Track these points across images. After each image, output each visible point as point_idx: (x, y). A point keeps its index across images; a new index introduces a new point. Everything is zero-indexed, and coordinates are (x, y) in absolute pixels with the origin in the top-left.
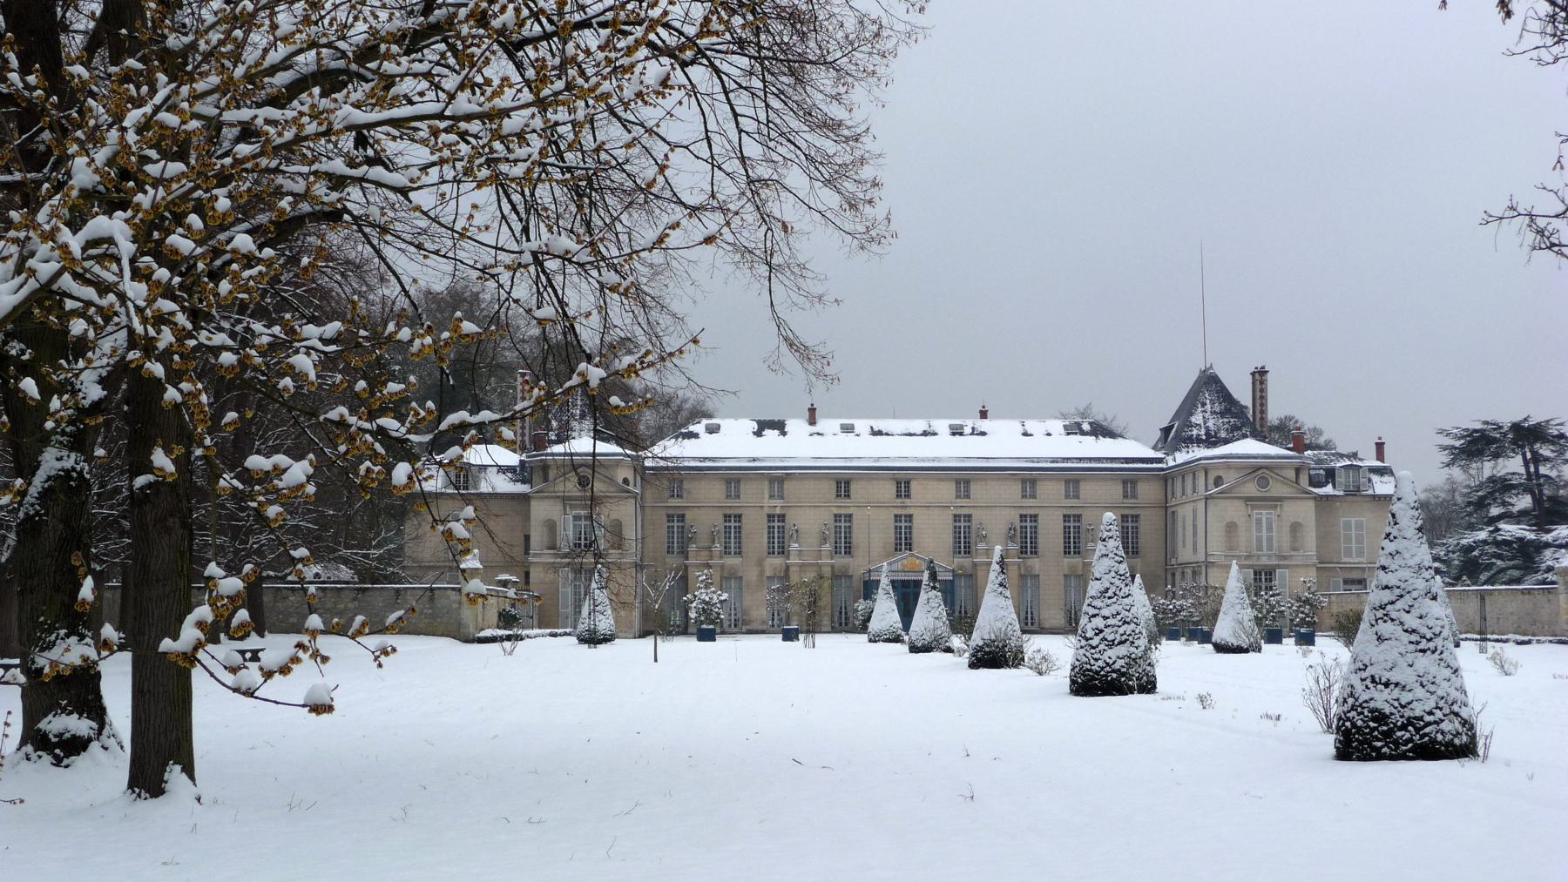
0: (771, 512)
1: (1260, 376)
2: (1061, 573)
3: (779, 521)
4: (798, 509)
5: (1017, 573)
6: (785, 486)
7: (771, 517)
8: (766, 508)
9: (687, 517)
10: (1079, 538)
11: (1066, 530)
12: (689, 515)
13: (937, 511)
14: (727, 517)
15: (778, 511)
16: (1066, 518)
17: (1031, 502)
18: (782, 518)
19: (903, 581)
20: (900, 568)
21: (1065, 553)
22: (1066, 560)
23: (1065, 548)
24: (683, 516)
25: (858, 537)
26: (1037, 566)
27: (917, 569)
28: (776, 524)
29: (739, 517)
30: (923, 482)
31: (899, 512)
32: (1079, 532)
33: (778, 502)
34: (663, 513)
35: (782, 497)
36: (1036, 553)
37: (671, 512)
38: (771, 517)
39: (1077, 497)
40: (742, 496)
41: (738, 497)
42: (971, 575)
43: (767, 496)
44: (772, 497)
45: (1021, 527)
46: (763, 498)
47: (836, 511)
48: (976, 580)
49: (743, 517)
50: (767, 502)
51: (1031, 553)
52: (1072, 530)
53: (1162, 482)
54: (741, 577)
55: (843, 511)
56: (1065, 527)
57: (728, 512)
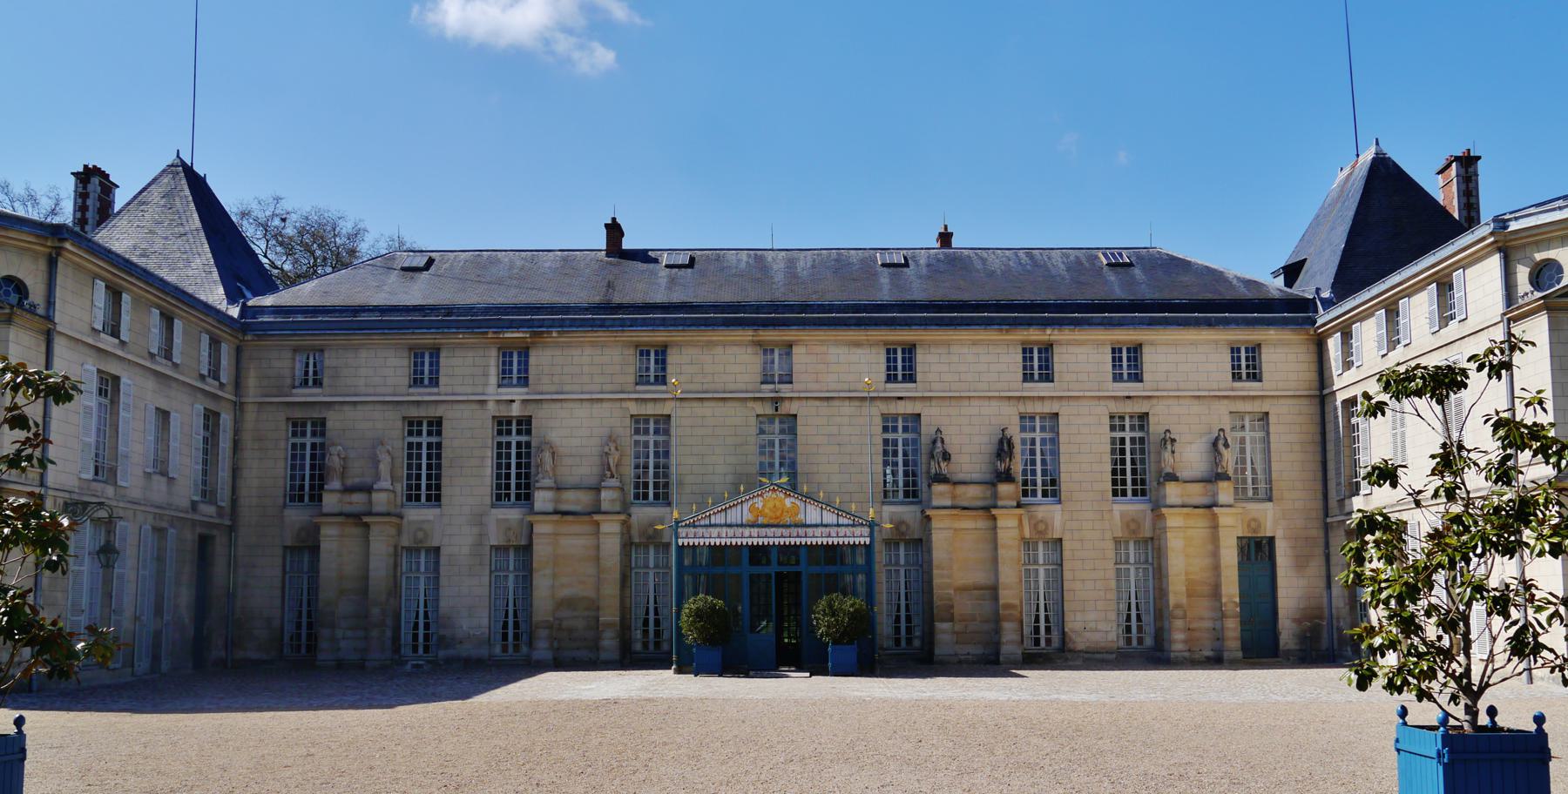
0: (503, 412)
1: (1467, 163)
2: (1108, 535)
3: (519, 432)
4: (558, 405)
5: (1015, 533)
6: (532, 360)
7: (503, 425)
8: (491, 406)
9: (329, 424)
10: (1143, 461)
11: (1118, 448)
12: (334, 421)
13: (847, 409)
14: (413, 425)
15: (516, 410)
16: (1116, 422)
17: (1042, 389)
18: (525, 424)
19: (754, 549)
20: (748, 517)
21: (1115, 493)
22: (1117, 507)
23: (1114, 482)
24: (323, 422)
25: (681, 462)
26: (1057, 522)
27: (787, 520)
28: (514, 439)
29: (436, 425)
30: (818, 349)
31: (768, 409)
32: (1142, 451)
33: (517, 393)
34: (281, 416)
35: (524, 381)
36: (1055, 494)
37: (298, 414)
38: (503, 425)
39: (1137, 378)
40: (442, 380)
41: (434, 382)
42: (921, 540)
43: (493, 380)
44: (505, 379)
45: (1023, 442)
46: (486, 385)
47: (634, 409)
48: (930, 551)
49: (446, 425)
50: (493, 391)
51: (1045, 494)
52: (1128, 446)
53: (1313, 348)
54: (437, 550)
55: (650, 409)
56: (1113, 441)
57: (414, 412)
